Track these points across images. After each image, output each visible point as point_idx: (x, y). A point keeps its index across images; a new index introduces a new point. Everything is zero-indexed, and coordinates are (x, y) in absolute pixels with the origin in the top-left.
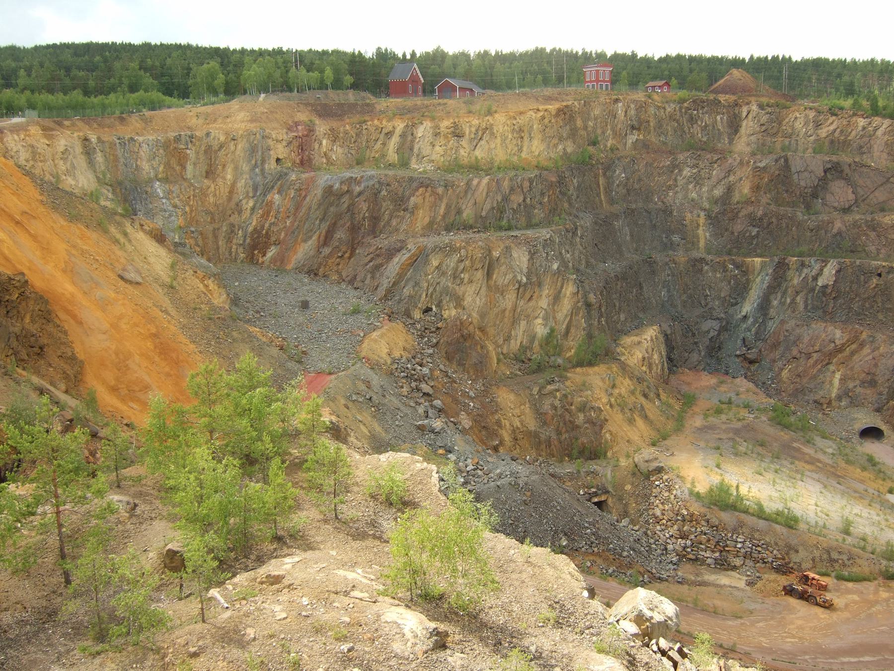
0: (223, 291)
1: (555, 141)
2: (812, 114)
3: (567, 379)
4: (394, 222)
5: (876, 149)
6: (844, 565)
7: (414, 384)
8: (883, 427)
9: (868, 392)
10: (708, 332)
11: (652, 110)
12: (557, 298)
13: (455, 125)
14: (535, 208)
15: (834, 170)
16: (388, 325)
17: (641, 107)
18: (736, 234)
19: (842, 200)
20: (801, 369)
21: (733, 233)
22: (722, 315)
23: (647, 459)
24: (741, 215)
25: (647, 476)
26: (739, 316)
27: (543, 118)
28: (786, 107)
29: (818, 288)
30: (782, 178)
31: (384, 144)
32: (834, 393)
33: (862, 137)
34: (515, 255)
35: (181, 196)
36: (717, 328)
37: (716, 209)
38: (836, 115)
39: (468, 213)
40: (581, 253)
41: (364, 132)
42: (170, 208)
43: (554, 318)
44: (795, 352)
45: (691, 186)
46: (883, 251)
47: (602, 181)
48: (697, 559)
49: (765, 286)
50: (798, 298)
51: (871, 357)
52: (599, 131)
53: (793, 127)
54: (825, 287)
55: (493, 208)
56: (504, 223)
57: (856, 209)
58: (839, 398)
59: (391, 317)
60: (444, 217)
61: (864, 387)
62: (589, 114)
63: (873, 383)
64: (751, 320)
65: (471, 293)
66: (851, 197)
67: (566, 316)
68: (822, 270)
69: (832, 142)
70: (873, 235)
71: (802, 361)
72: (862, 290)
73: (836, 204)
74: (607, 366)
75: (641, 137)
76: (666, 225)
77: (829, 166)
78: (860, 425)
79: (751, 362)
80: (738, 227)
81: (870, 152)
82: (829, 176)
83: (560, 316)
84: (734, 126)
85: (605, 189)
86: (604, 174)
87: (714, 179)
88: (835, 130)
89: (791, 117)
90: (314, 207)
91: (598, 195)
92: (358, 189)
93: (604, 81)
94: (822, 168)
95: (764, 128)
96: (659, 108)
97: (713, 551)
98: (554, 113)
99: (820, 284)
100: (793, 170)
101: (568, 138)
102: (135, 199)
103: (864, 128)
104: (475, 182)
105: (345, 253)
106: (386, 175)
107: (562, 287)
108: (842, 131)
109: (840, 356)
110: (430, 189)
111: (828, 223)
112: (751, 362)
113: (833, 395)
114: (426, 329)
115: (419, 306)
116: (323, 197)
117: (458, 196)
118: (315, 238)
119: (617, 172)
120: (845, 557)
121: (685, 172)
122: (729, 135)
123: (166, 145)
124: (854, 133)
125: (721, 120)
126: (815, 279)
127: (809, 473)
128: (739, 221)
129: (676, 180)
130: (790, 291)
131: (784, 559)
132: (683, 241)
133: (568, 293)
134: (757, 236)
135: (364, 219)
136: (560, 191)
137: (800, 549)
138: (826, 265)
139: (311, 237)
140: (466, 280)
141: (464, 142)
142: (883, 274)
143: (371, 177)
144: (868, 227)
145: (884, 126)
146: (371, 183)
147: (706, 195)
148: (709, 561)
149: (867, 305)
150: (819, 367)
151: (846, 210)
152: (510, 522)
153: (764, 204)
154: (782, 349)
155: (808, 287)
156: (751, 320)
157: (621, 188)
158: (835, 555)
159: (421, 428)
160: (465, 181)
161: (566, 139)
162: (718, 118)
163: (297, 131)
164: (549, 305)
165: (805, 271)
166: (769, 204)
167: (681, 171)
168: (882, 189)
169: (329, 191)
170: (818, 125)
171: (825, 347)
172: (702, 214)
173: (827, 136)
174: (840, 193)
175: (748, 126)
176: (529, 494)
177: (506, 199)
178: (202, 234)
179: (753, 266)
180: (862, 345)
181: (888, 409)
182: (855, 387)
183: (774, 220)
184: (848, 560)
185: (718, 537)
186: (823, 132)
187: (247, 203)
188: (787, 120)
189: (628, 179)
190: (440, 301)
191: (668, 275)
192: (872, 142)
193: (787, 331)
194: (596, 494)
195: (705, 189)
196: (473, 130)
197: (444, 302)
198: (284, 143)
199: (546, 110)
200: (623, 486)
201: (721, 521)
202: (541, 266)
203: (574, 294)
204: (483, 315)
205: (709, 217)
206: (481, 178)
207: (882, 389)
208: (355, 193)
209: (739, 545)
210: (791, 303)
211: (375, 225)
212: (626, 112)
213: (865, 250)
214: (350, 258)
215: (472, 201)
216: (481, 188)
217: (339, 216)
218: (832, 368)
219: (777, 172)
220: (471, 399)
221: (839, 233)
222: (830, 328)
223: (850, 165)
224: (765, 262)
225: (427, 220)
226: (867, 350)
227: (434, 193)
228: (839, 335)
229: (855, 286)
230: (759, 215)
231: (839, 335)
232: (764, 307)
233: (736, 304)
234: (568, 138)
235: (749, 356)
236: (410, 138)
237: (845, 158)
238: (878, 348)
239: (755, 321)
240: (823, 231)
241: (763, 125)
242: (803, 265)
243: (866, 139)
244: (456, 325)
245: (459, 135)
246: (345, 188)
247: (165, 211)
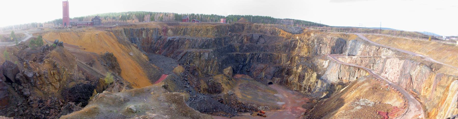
15: (261, 37)
16: (179, 66)
59: (180, 65)
78: (268, 82)
80: (244, 48)
153: (249, 43)
174: (262, 40)
204: (199, 66)
231: (263, 66)
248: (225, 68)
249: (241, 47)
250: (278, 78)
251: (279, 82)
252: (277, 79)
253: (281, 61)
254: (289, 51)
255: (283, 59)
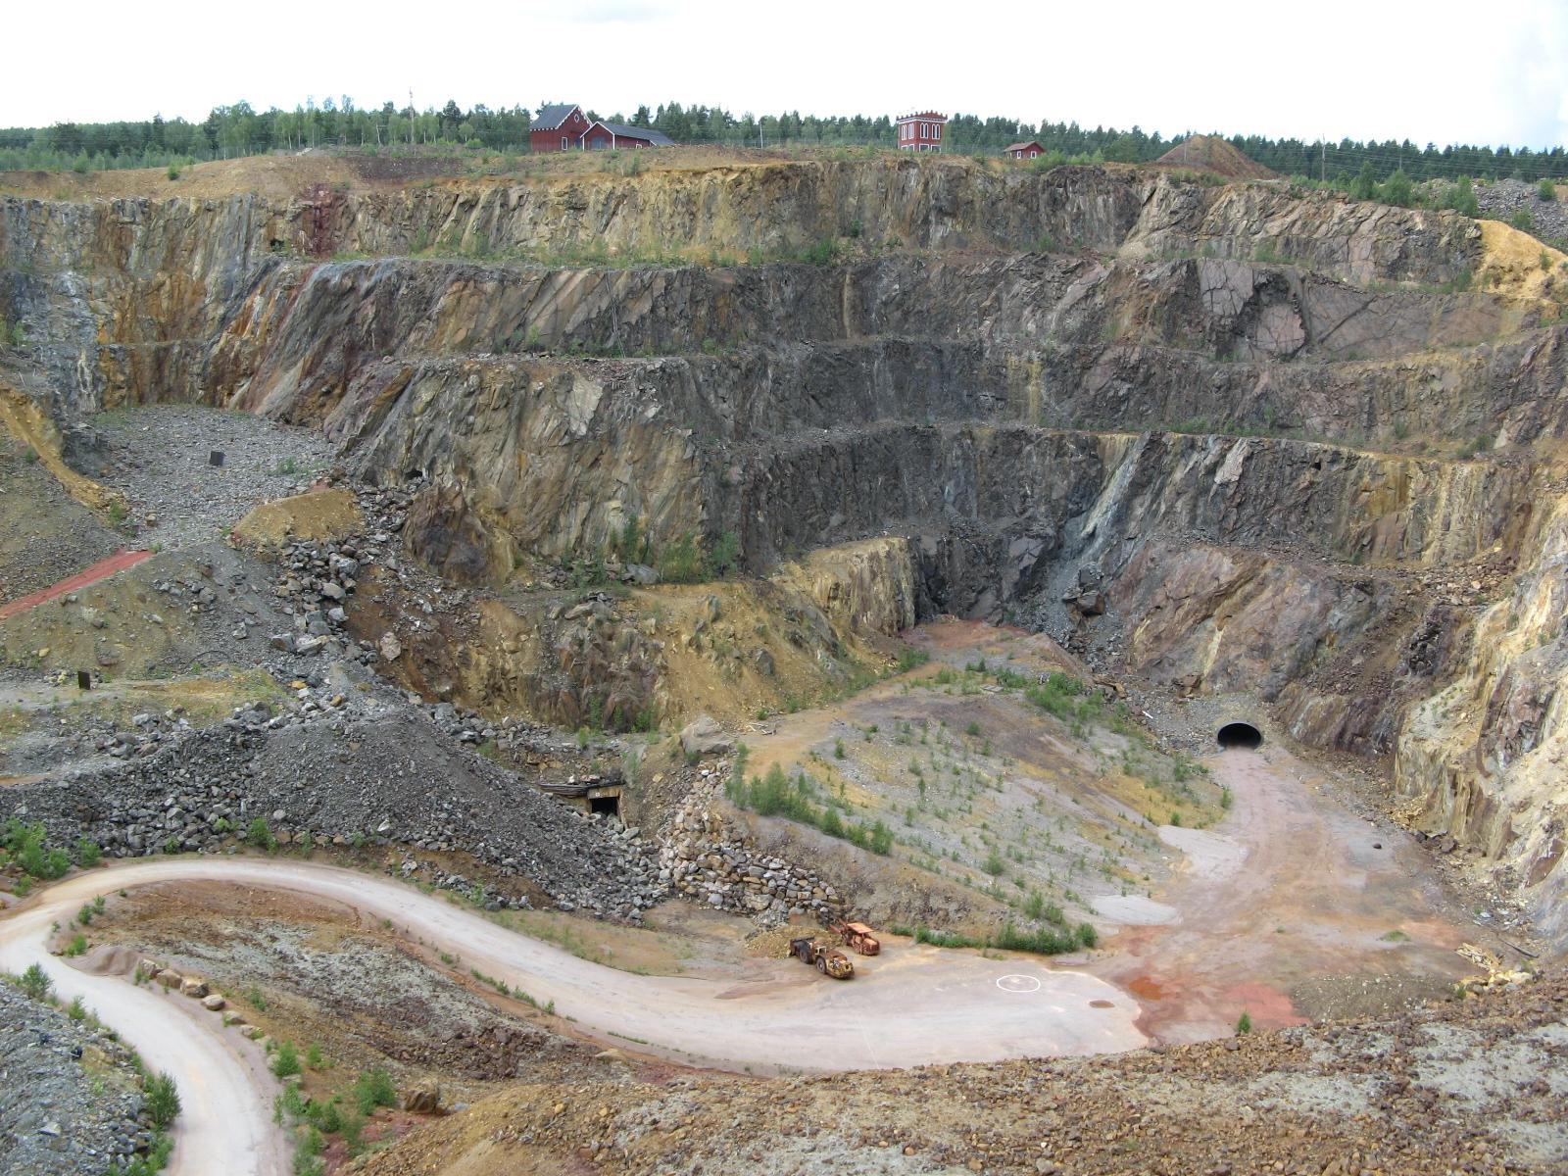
0: (50, 423)
1: (761, 222)
2: (1258, 198)
3: (626, 597)
4: (412, 338)
5: (1356, 257)
6: (946, 919)
7: (306, 581)
8: (1265, 726)
9: (1257, 666)
10: (1020, 558)
11: (978, 183)
12: (647, 468)
13: (573, 190)
14: (673, 324)
15: (1272, 289)
17: (957, 179)
18: (1092, 393)
19: (1282, 339)
20: (1163, 626)
21: (1087, 391)
22: (1050, 531)
23: (701, 731)
24: (1105, 358)
25: (695, 760)
26: (1082, 535)
27: (738, 183)
28: (1217, 184)
29: (1215, 487)
30: (1184, 297)
31: (457, 221)
32: (1208, 667)
33: (1337, 233)
34: (579, 388)
35: (109, 295)
36: (1036, 552)
37: (1064, 349)
38: (1301, 198)
39: (539, 323)
40: (769, 405)
41: (428, 202)
42: (87, 313)
43: (644, 501)
44: (1160, 598)
45: (1027, 312)
46: (1333, 426)
47: (847, 293)
48: (696, 895)
49: (1126, 483)
50: (1179, 504)
51: (1269, 605)
52: (868, 214)
53: (1226, 219)
54: (1224, 485)
55: (588, 321)
56: (610, 344)
57: (1305, 355)
58: (1213, 677)
60: (493, 331)
61: (1253, 658)
62: (848, 186)
63: (1264, 651)
64: (1100, 540)
65: (488, 449)
66: (1299, 334)
67: (667, 499)
68: (1223, 456)
69: (1287, 243)
70: (1320, 397)
71: (1168, 612)
72: (1286, 492)
73: (1272, 347)
74: (725, 585)
75: (959, 228)
76: (970, 377)
77: (1263, 280)
78: (1221, 723)
79: (1089, 613)
80: (1096, 379)
81: (1347, 261)
82: (1265, 298)
83: (654, 498)
84: (1128, 215)
85: (854, 307)
86: (855, 283)
87: (1067, 301)
88: (1294, 223)
89: (1224, 199)
90: (301, 314)
91: (839, 316)
92: (365, 285)
93: (930, 141)
94: (1250, 284)
95: (1176, 218)
96: (992, 181)
97: (724, 883)
98: (759, 175)
99: (1218, 479)
100: (1204, 286)
101: (793, 219)
102: (21, 294)
103: (1342, 220)
104: (563, 278)
105: (333, 387)
106: (413, 263)
107: (660, 449)
108: (1305, 224)
109: (1226, 603)
110: (472, 283)
111: (1249, 377)
112: (1089, 613)
113: (1206, 671)
114: (392, 503)
115: (395, 466)
116: (313, 297)
117: (523, 298)
118: (300, 364)
119: (885, 281)
120: (952, 907)
121: (1017, 287)
122: (1118, 228)
123: (99, 217)
124: (1324, 227)
125: (1102, 206)
126: (1212, 471)
127: (1027, 782)
128: (1099, 370)
129: (997, 299)
130: (1167, 491)
131: (842, 902)
132: (1000, 404)
133: (672, 460)
134: (1126, 398)
135: (369, 332)
136: (743, 302)
137: (879, 888)
138: (1230, 448)
139: (295, 364)
140: (478, 428)
141: (586, 218)
142: (1324, 465)
143: (389, 266)
144: (1314, 384)
145: (1375, 217)
146: (388, 274)
147: (1053, 326)
148: (713, 898)
149: (1293, 519)
150: (1191, 622)
151: (1288, 357)
152: (300, 785)
154: (1141, 591)
155: (1200, 486)
156: (1100, 540)
157: (892, 307)
158: (935, 902)
159: (278, 645)
160: (542, 275)
161: (788, 223)
162: (1100, 200)
163: (316, 198)
164: (634, 477)
165: (1195, 457)
166: (1155, 343)
167: (1009, 284)
168: (1353, 321)
169: (323, 285)
170: (1267, 214)
171: (1204, 588)
172: (1035, 355)
173: (1280, 233)
174: (1281, 326)
175: (1152, 214)
176: (355, 746)
177: (618, 307)
178: (132, 356)
179: (1113, 447)
180: (1262, 585)
181: (1285, 697)
182: (1238, 657)
183: (1155, 369)
184: (957, 911)
185: (740, 859)
186: (1274, 227)
187: (216, 309)
188: (1216, 205)
189: (905, 293)
190: (433, 462)
191: (957, 458)
192: (1352, 243)
193: (1152, 560)
194: (595, 785)
195: (1053, 316)
196: (602, 198)
197: (439, 461)
198: (289, 217)
199: (744, 171)
200: (649, 775)
201: (752, 833)
202: (621, 410)
203: (685, 461)
205: (1047, 362)
206: (576, 271)
207: (1279, 661)
208: (362, 291)
209: (768, 875)
210: (1166, 513)
211: (385, 338)
212: (926, 184)
213: (1304, 424)
214: (341, 396)
215: (551, 308)
216: (572, 286)
217: (336, 329)
218: (1210, 624)
219: (1173, 289)
220: (424, 615)
221: (1264, 395)
222: (1217, 555)
223: (1303, 281)
224: (1133, 442)
225: (461, 335)
226: (1267, 593)
227: (478, 292)
228: (1224, 566)
229: (1275, 485)
230: (1132, 362)
232: (1121, 517)
233: (1079, 513)
234: (793, 219)
235: (1083, 602)
236: (497, 211)
237: (1295, 271)
238: (1283, 590)
239: (1107, 543)
240: (1239, 391)
241: (1174, 213)
242: (1193, 446)
243: (1342, 239)
244: (432, 497)
245: (578, 208)
246: (348, 283)
247: (74, 316)
248: (829, 544)
249: (1065, 371)
250: (1327, 686)
251: (1333, 730)
252: (1316, 702)
253: (1422, 527)
254: (1525, 439)
255: (1436, 521)
